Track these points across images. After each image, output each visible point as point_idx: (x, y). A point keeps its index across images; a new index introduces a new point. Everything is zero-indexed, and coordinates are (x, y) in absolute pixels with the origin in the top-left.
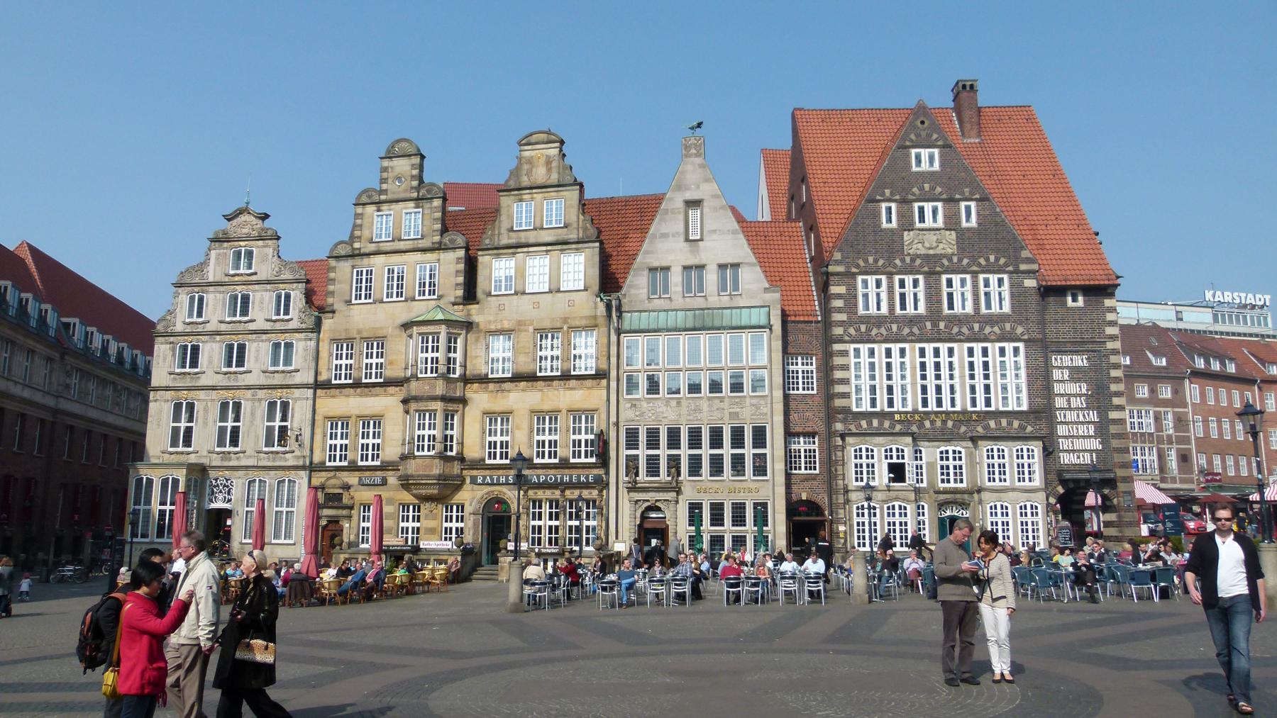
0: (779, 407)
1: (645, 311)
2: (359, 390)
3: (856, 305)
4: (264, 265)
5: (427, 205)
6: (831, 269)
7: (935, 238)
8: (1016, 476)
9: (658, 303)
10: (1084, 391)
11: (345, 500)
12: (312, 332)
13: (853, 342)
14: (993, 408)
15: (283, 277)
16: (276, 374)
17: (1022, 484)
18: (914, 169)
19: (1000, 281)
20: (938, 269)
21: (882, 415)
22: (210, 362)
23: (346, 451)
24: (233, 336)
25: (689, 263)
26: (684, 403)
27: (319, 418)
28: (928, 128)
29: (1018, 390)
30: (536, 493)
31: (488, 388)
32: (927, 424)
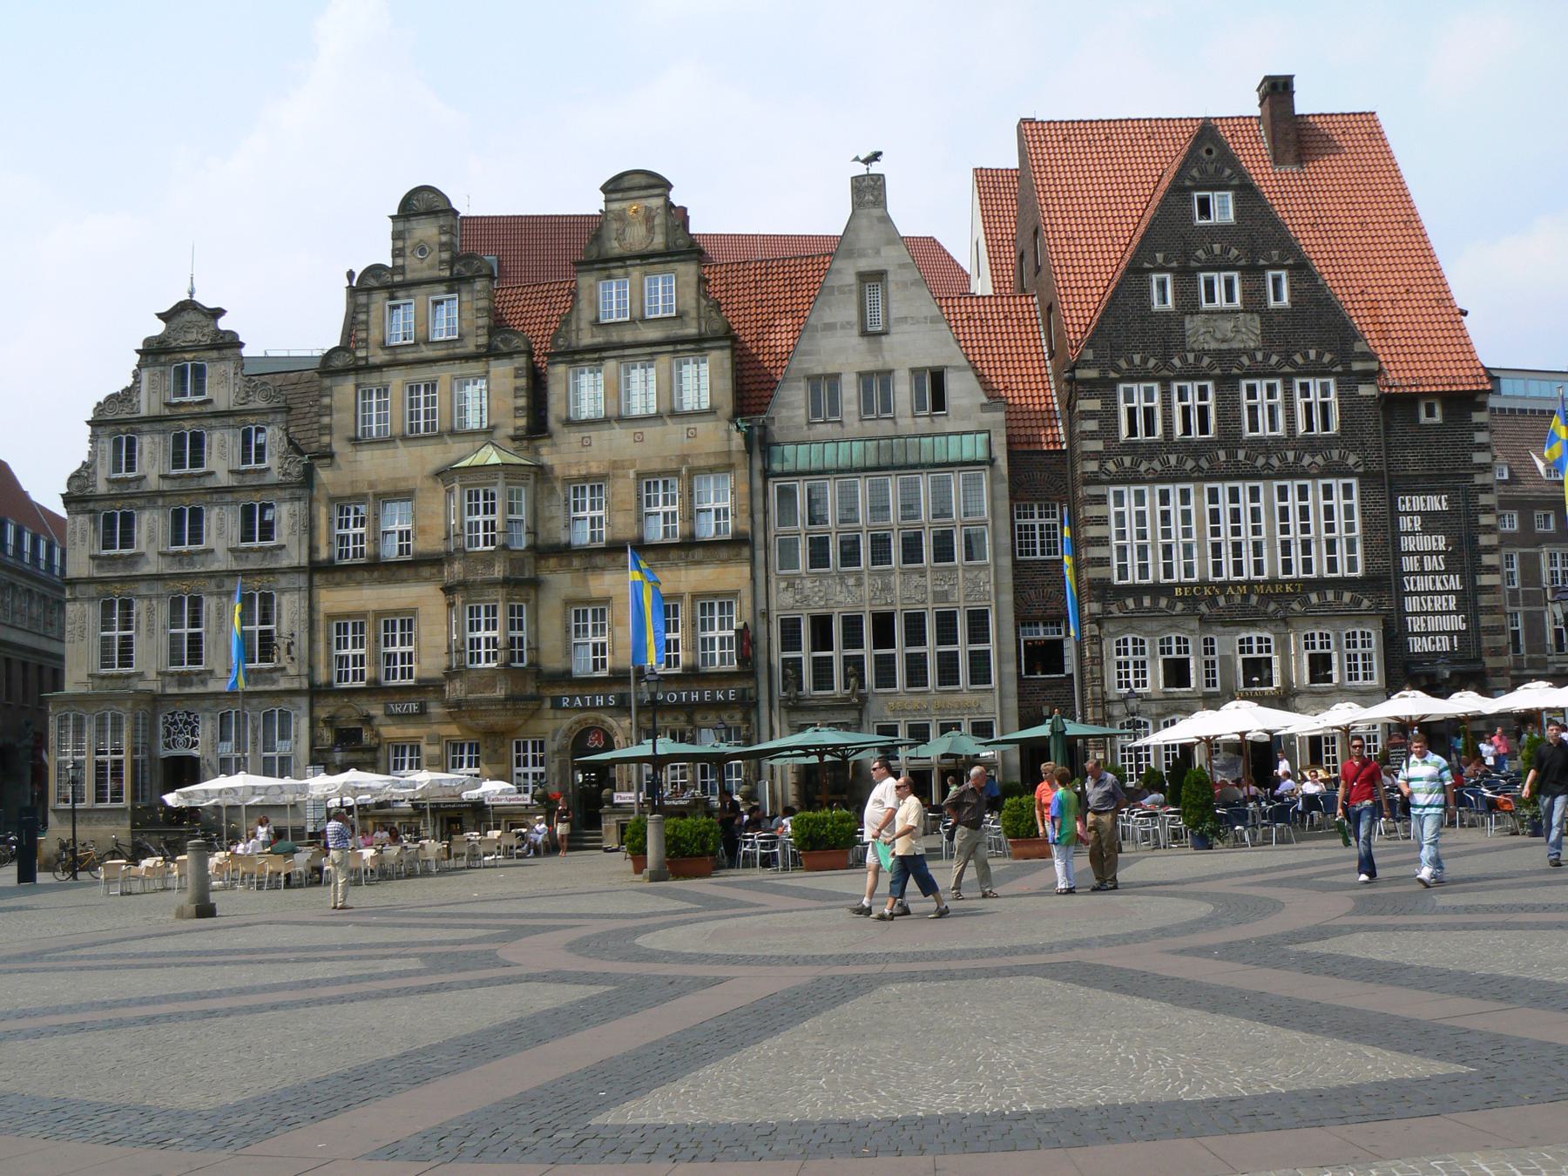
1: (803, 443)
2: (376, 575)
3: (1117, 428)
5: (464, 288)
8: (1346, 672)
10: (1442, 547)
11: (366, 736)
14: (1314, 575)
15: (251, 406)
18: (1199, 222)
20: (1235, 371)
21: (1156, 590)
22: (151, 539)
25: (870, 365)
26: (866, 580)
27: (315, 617)
29: (1351, 545)
31: (570, 565)
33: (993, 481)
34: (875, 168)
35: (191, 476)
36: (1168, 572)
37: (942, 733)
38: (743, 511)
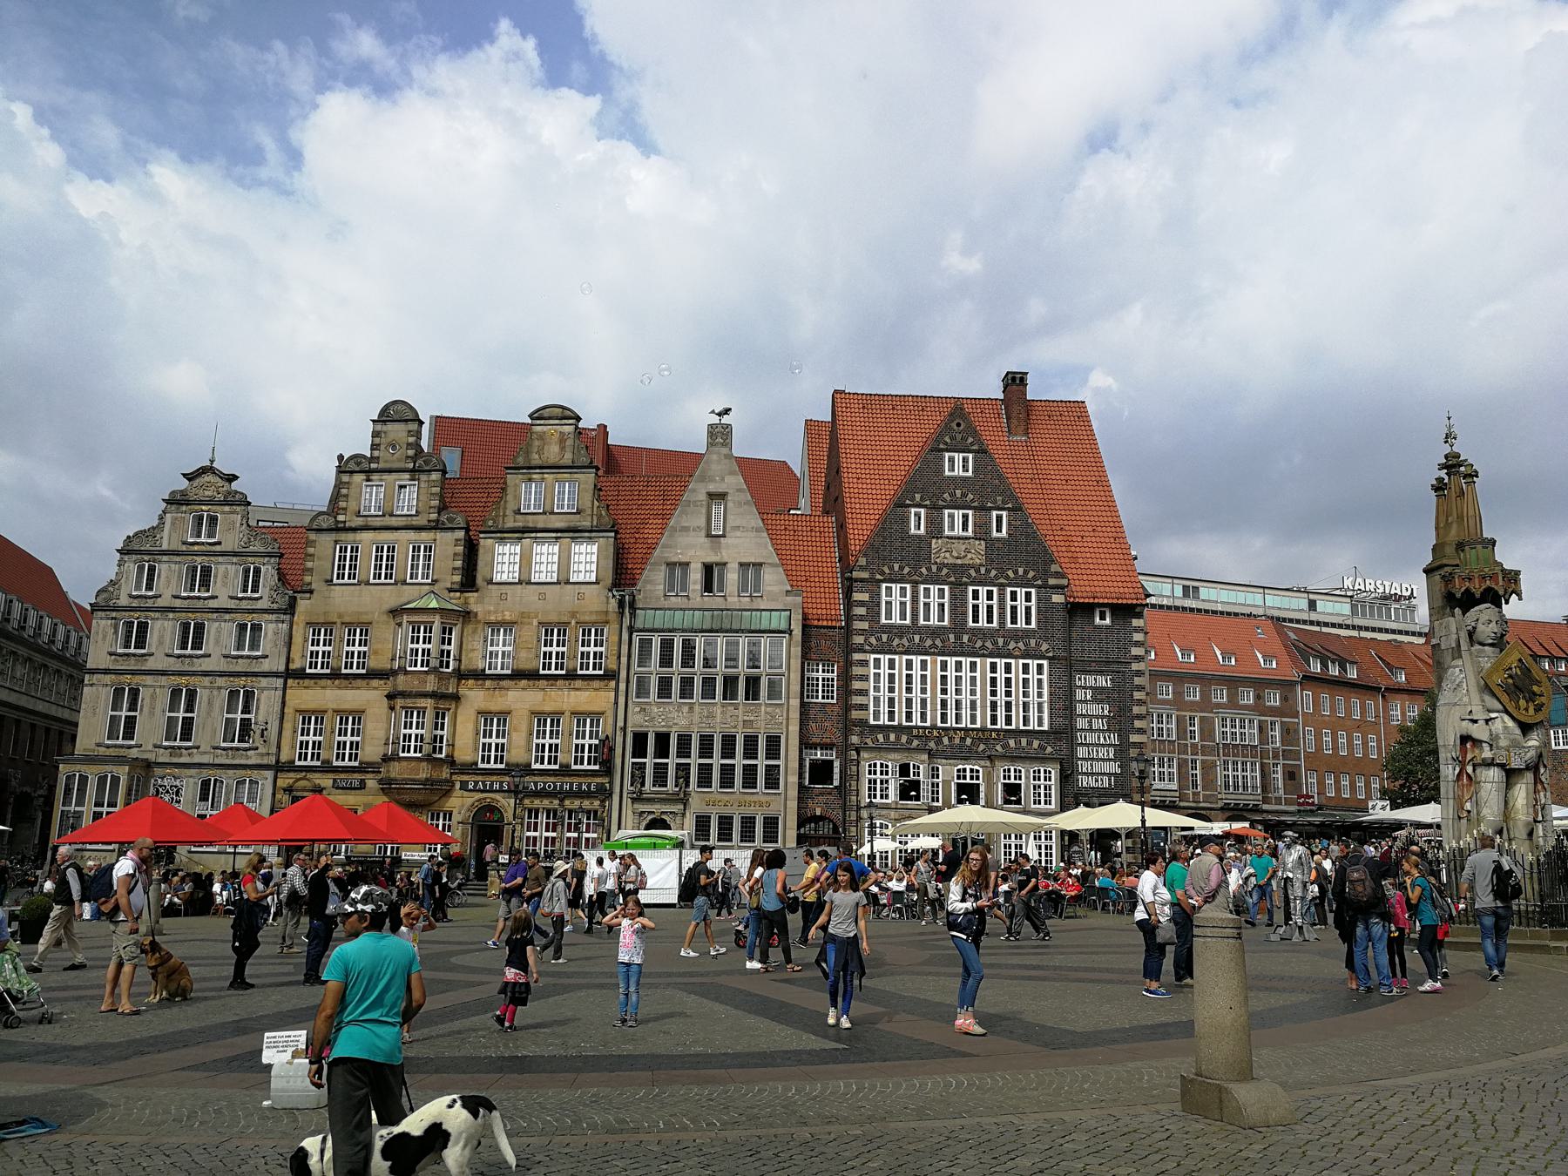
0: (795, 715)
1: (660, 609)
2: (337, 682)
3: (878, 614)
4: (230, 534)
5: (423, 477)
6: (855, 574)
7: (963, 547)
9: (674, 601)
12: (284, 614)
13: (873, 652)
16: (240, 660)
17: (1037, 806)
18: (947, 473)
19: (1028, 595)
22: (161, 643)
23: (319, 749)
24: (190, 615)
26: (696, 707)
29: (1040, 705)
32: (946, 741)
34: (726, 419)
35: (199, 598)
36: (909, 716)
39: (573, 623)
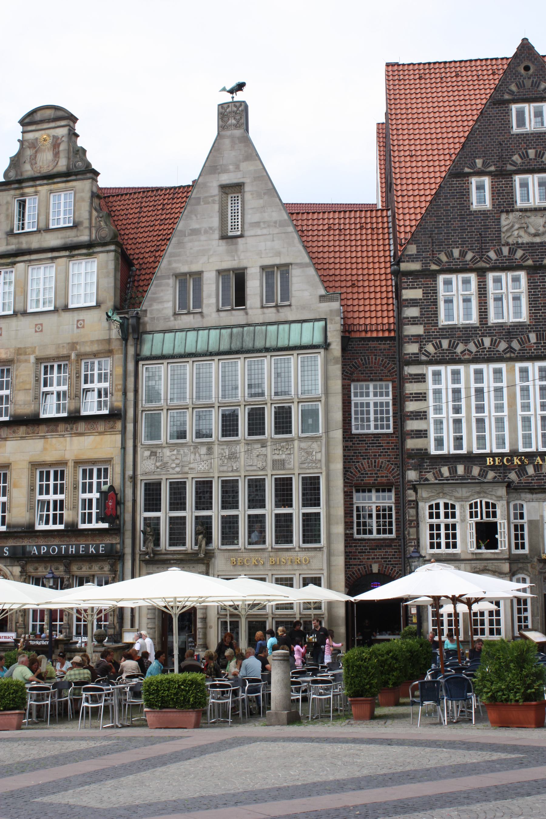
1: (170, 331)
3: (436, 314)
6: (404, 266)
9: (187, 321)
18: (515, 130)
26: (216, 449)
28: (534, 75)
30: (37, 569)
32: (531, 470)
33: (326, 363)
37: (305, 585)
38: (118, 390)
39: (73, 356)
